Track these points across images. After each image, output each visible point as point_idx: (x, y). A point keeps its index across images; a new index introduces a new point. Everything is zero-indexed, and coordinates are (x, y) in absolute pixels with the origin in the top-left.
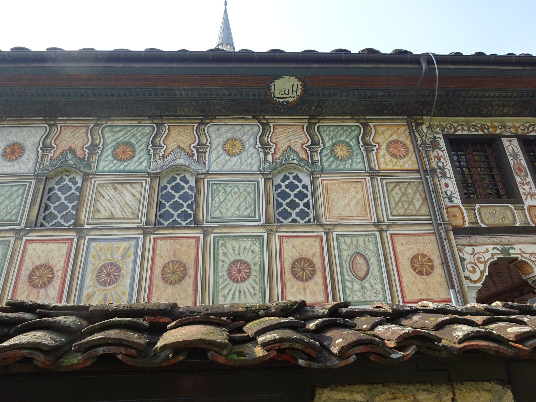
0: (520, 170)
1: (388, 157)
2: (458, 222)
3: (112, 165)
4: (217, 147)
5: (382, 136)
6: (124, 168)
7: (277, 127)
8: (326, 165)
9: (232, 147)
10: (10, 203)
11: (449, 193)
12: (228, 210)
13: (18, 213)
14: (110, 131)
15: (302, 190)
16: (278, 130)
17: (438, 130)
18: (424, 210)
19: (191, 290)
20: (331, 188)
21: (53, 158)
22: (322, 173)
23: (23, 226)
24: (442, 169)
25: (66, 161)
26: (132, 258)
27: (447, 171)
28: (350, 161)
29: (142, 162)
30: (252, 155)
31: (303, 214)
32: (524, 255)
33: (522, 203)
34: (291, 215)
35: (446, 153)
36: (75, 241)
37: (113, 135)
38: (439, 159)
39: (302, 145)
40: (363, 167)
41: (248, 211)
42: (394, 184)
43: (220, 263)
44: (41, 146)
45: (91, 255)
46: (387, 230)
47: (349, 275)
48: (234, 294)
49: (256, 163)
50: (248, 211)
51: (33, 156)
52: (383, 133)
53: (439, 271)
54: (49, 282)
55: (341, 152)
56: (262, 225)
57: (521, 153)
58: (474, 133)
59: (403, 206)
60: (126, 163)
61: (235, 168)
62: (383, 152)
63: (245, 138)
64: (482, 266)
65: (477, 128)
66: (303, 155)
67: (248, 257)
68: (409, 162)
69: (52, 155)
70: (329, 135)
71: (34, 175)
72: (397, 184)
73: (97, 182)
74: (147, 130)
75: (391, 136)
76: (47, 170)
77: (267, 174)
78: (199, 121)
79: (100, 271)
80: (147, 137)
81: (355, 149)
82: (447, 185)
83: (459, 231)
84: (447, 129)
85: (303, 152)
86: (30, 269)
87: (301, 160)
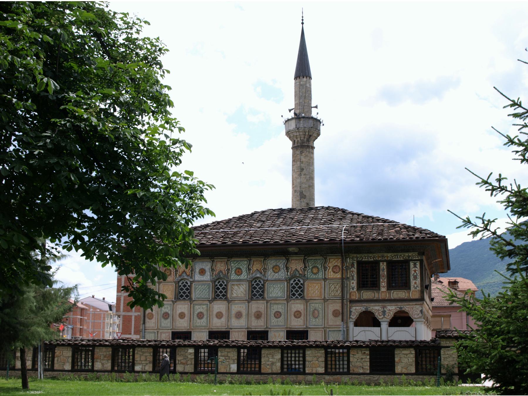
0: (383, 276)
1: (332, 273)
2: (353, 298)
8: (309, 276)
9: (276, 269)
16: (293, 261)
18: (340, 295)
31: (300, 295)
33: (380, 290)
51: (209, 274)
55: (315, 271)
62: (330, 270)
64: (357, 314)
67: (280, 310)
74: (246, 262)
82: (353, 283)
83: (352, 301)
87: (300, 274)
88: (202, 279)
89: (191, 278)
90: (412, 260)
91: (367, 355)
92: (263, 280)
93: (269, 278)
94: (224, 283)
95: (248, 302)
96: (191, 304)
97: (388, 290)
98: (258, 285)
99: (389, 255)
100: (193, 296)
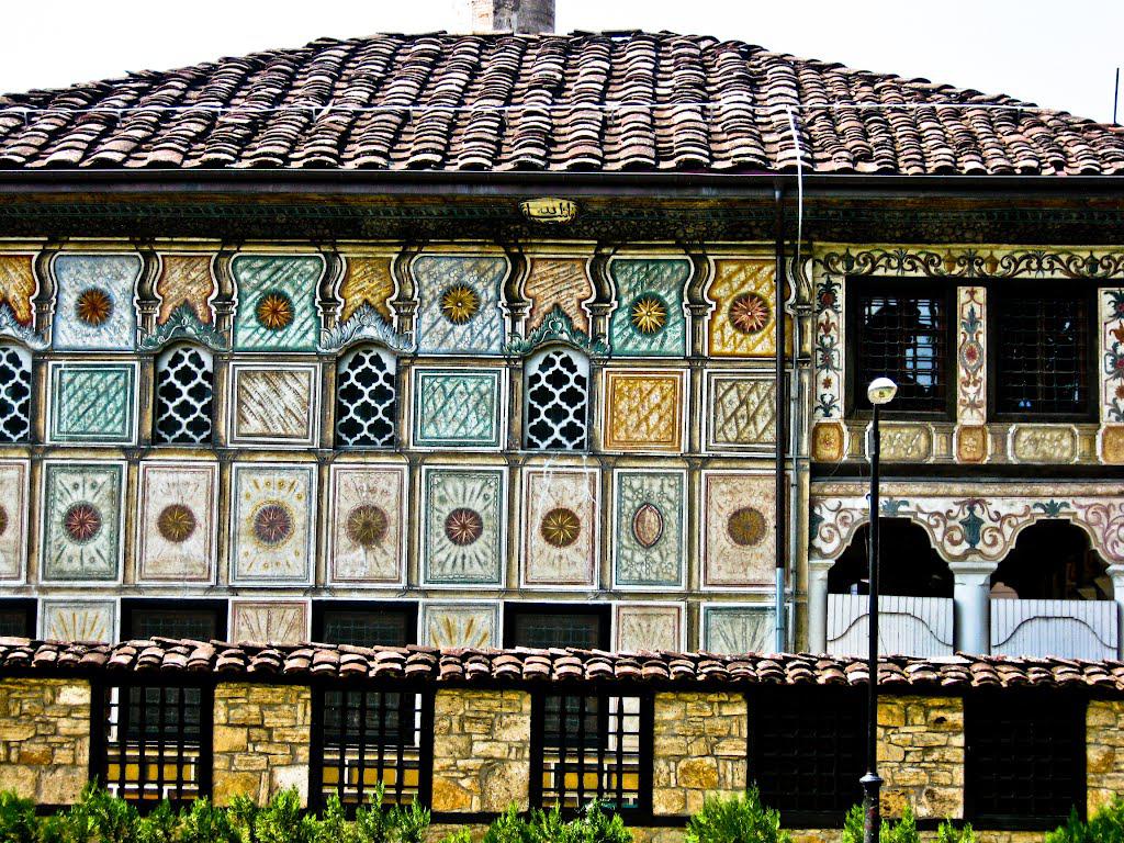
0: (971, 355)
1: (729, 330)
2: (829, 453)
3: (257, 336)
4: (430, 304)
5: (727, 285)
7: (538, 263)
8: (618, 342)
10: (109, 402)
11: (827, 399)
13: (123, 420)
14: (248, 267)
15: (576, 386)
16: (541, 269)
17: (840, 267)
20: (621, 390)
21: (162, 322)
22: (610, 359)
23: (134, 442)
24: (827, 350)
25: (183, 329)
27: (835, 354)
28: (660, 336)
29: (307, 332)
30: (490, 322)
31: (571, 432)
32: (920, 516)
33: (954, 420)
34: (551, 431)
35: (842, 316)
36: (217, 469)
37: (253, 277)
38: (827, 330)
39: (580, 301)
40: (680, 350)
41: (481, 427)
42: (730, 384)
44: (137, 297)
46: (703, 467)
47: (629, 539)
48: (455, 562)
49: (497, 337)
50: (481, 427)
51: (128, 317)
52: (729, 278)
53: (769, 542)
55: (648, 317)
56: (502, 454)
57: (984, 322)
58: (908, 274)
59: (737, 424)
60: (280, 334)
61: (461, 346)
62: (722, 317)
63: (479, 287)
64: (844, 531)
65: (917, 263)
66: (579, 323)
67: (477, 505)
68: (766, 339)
70: (629, 281)
72: (735, 383)
73: (237, 369)
74: (310, 267)
75: (743, 284)
77: (515, 360)
78: (399, 249)
80: (311, 282)
81: (672, 311)
82: (827, 383)
83: (821, 470)
84: (859, 264)
85: (580, 316)
87: (575, 332)
88: (95, 343)
90: (1106, 282)
91: (954, 730)
92: (393, 353)
93: (427, 346)
94: (200, 364)
95: (322, 463)
96: (34, 464)
97: (991, 419)
98: (367, 377)
99: (1001, 252)
100: (48, 431)
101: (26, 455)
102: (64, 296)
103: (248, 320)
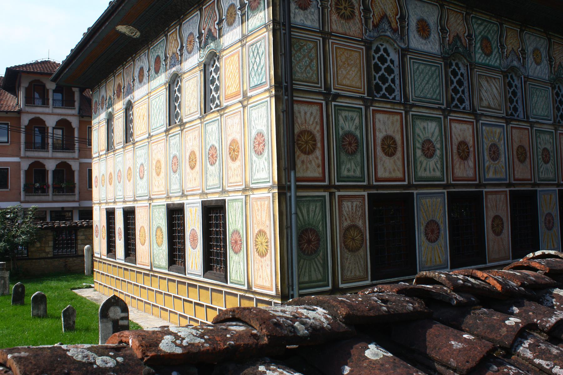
3: (482, 58)
6: (489, 62)
12: (539, 110)
13: (440, 93)
14: (476, 22)
19: (529, 167)
21: (450, 43)
25: (457, 48)
26: (502, 142)
36: (475, 123)
43: (539, 150)
44: (439, 28)
45: (484, 136)
51: (437, 37)
54: (468, 155)
60: (489, 58)
63: (542, 49)
67: (548, 147)
69: (447, 39)
71: (442, 58)
74: (496, 29)
76: (448, 54)
79: (490, 151)
86: (457, 144)
89: (402, 38)
96: (407, 113)
101: (402, 108)
102: (411, 19)
103: (478, 49)
